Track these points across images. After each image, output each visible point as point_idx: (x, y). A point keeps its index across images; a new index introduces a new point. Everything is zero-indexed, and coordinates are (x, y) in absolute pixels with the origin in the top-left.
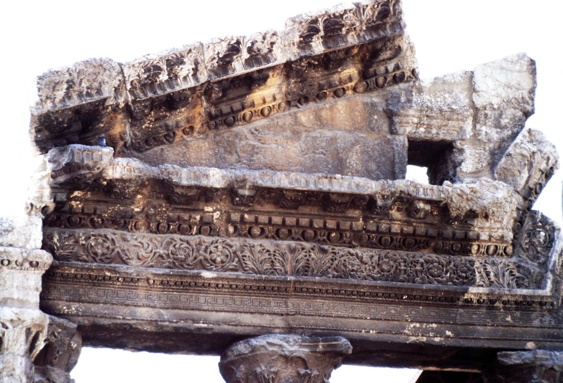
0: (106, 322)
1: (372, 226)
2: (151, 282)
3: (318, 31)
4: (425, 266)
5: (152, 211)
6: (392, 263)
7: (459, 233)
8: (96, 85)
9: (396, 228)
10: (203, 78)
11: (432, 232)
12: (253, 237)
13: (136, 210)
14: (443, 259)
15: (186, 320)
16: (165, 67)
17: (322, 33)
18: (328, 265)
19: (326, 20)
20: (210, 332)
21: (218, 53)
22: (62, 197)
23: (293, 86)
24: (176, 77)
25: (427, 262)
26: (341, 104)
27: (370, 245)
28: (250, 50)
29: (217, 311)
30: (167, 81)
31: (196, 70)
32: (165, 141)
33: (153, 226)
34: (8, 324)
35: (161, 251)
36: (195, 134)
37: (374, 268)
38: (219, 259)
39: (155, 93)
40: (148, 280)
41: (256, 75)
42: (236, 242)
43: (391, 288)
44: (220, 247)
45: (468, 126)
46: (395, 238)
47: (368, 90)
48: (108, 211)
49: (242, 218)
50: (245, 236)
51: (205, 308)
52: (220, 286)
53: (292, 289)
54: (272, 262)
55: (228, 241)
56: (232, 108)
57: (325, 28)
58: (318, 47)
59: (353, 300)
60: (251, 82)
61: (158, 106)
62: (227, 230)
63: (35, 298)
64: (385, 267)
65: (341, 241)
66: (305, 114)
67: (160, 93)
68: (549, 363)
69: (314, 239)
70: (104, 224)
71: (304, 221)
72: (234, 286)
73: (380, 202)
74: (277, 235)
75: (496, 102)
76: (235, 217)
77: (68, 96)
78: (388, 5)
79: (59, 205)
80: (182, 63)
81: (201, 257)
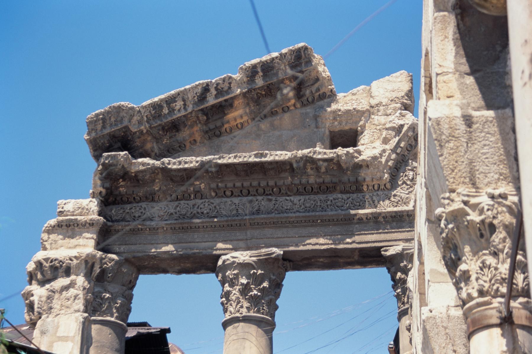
0: (140, 255)
1: (296, 181)
2: (165, 229)
3: (257, 72)
4: (333, 201)
6: (312, 202)
7: (352, 179)
8: (119, 119)
9: (312, 180)
10: (190, 110)
11: (335, 180)
12: (227, 197)
13: (156, 189)
14: (345, 196)
15: (186, 249)
16: (165, 105)
17: (261, 74)
18: (272, 207)
19: (262, 66)
20: (201, 255)
21: (196, 93)
23: (253, 108)
24: (174, 110)
25: (334, 199)
26: (287, 116)
27: (298, 193)
28: (216, 89)
29: (205, 242)
30: (168, 113)
31: (185, 105)
32: (180, 150)
34: (73, 259)
35: (172, 211)
36: (198, 144)
37: (301, 206)
38: (205, 212)
39: (162, 121)
41: (224, 104)
42: (217, 201)
43: (309, 216)
44: (207, 205)
46: (313, 187)
47: (303, 105)
48: (141, 192)
49: (217, 186)
50: (222, 197)
51: (197, 241)
52: (205, 227)
53: (248, 224)
54: (237, 210)
55: (212, 201)
56: (216, 126)
57: (263, 70)
58: (260, 82)
59: (287, 227)
60: (222, 109)
61: (167, 127)
62: (211, 195)
63: (92, 243)
64: (308, 205)
65: (280, 193)
69: (264, 193)
70: (141, 201)
71: (255, 183)
72: (213, 226)
73: (295, 165)
74: (241, 194)
75: (385, 101)
77: (104, 127)
78: (300, 52)
80: (176, 102)
81: (195, 212)
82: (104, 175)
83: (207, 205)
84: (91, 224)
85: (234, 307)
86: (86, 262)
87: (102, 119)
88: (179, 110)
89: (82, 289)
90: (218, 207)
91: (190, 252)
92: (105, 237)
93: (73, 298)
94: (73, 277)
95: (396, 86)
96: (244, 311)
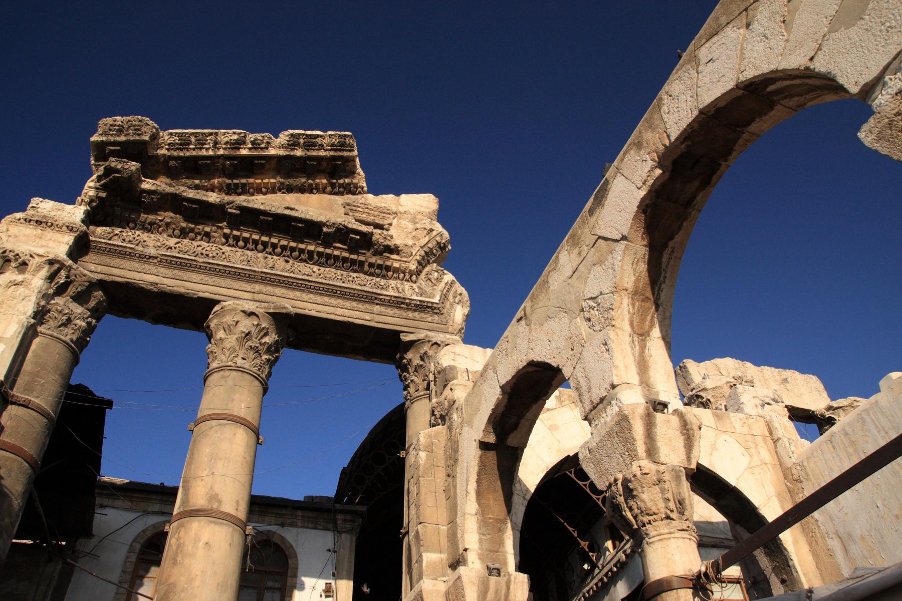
5: (168, 220)
9: (337, 253)
33: (170, 231)
38: (211, 255)
40: (156, 258)
42: (226, 249)
50: (233, 246)
58: (299, 153)
67: (188, 154)
68: (434, 340)
73: (325, 229)
83: (214, 249)
84: (71, 229)
85: (227, 355)
86: (51, 262)
87: (119, 126)
88: (207, 149)
89: (36, 291)
90: (227, 254)
91: (183, 290)
92: (81, 247)
93: (21, 298)
94: (27, 276)
95: (425, 203)
96: (240, 362)
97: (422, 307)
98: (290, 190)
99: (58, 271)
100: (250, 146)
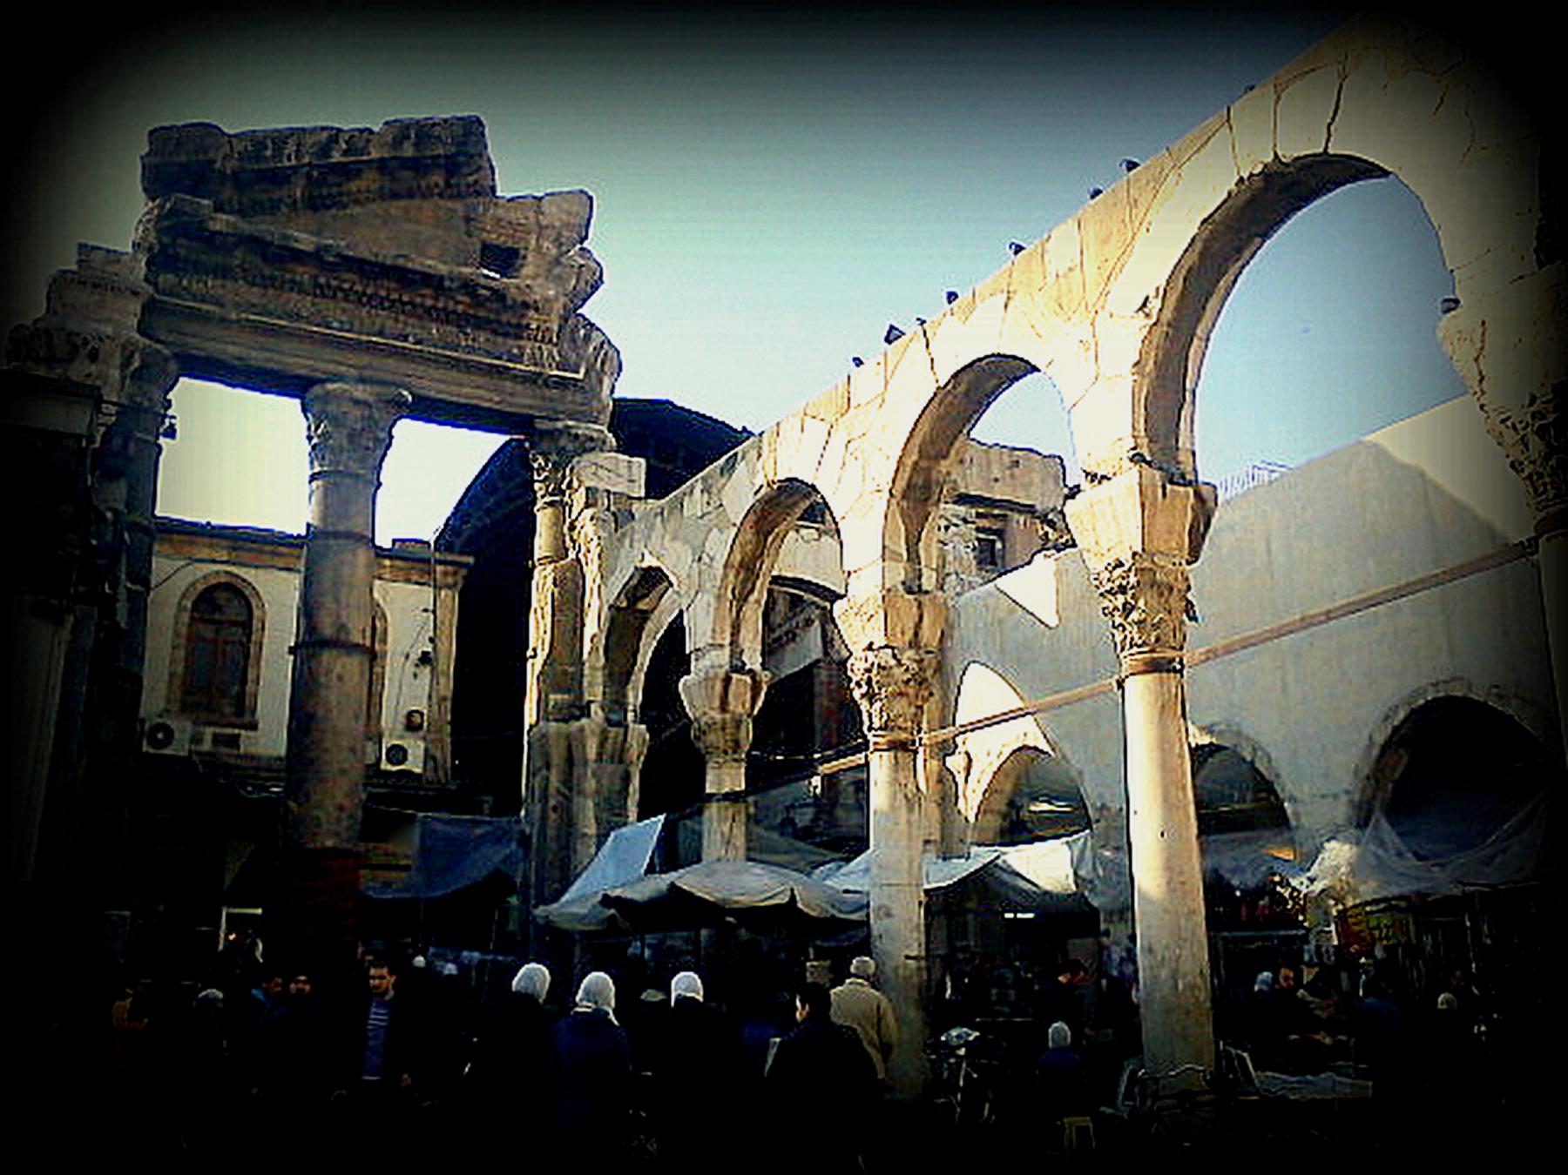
22: (166, 240)
26: (427, 205)
31: (298, 151)
45: (533, 242)
58: (408, 151)
60: (346, 171)
66: (395, 208)
73: (447, 283)
76: (322, 280)
79: (164, 247)
82: (165, 223)
97: (562, 383)
98: (395, 196)
99: (132, 354)
100: (344, 146)
